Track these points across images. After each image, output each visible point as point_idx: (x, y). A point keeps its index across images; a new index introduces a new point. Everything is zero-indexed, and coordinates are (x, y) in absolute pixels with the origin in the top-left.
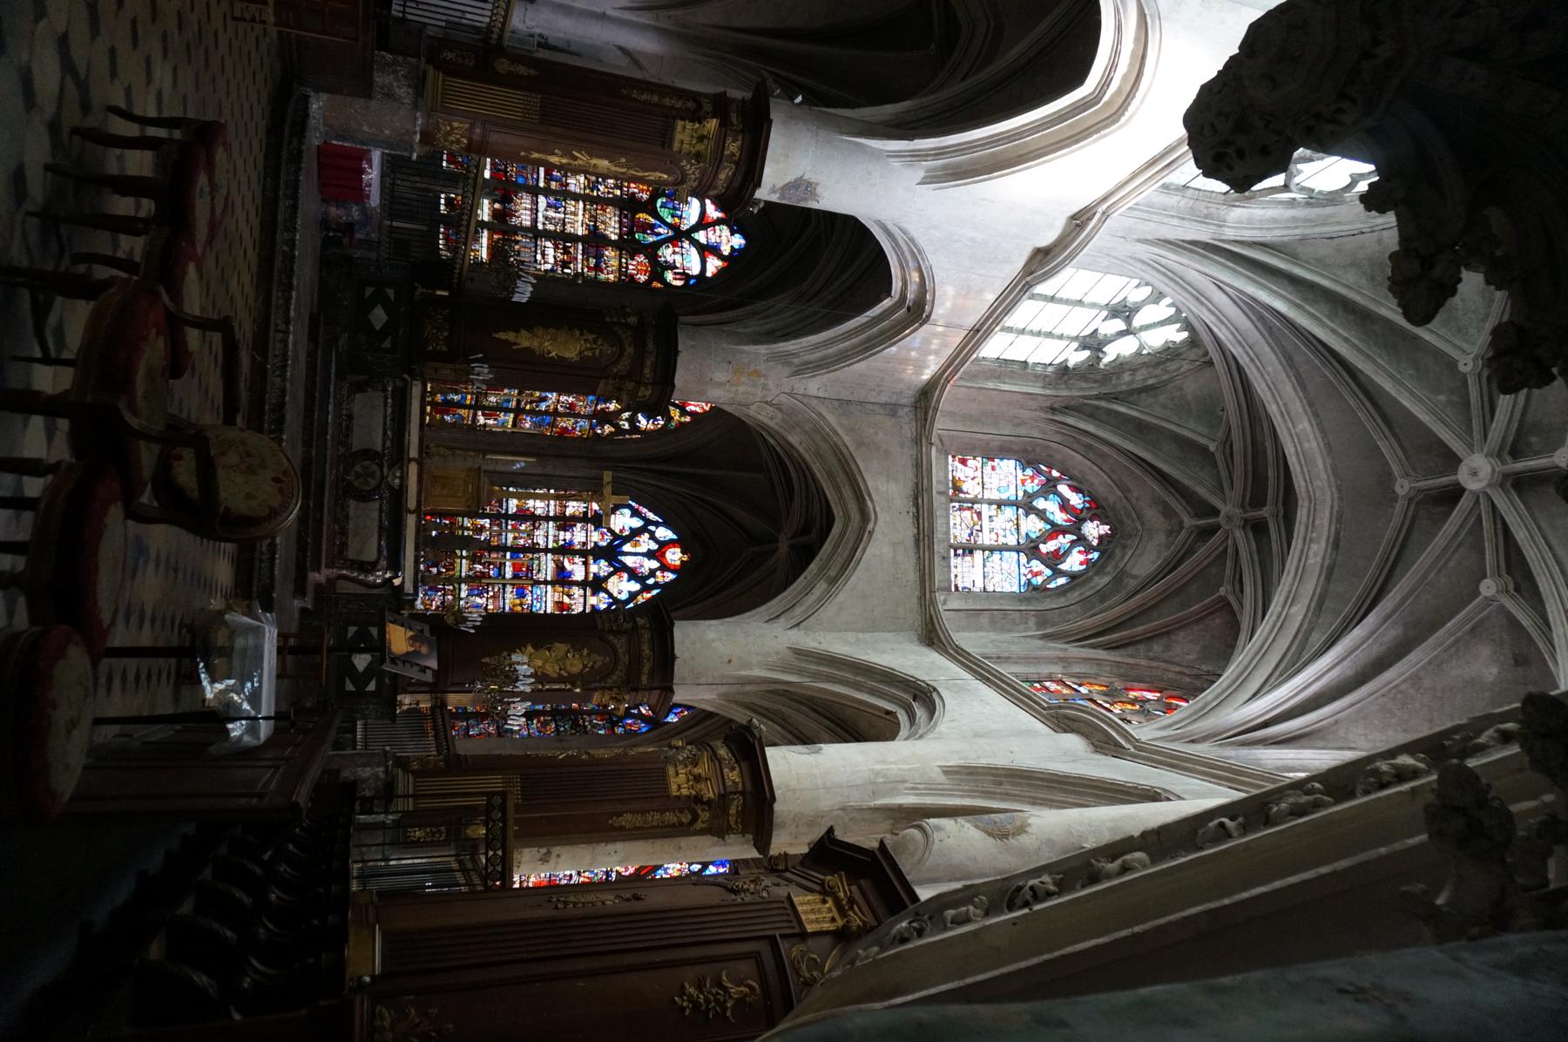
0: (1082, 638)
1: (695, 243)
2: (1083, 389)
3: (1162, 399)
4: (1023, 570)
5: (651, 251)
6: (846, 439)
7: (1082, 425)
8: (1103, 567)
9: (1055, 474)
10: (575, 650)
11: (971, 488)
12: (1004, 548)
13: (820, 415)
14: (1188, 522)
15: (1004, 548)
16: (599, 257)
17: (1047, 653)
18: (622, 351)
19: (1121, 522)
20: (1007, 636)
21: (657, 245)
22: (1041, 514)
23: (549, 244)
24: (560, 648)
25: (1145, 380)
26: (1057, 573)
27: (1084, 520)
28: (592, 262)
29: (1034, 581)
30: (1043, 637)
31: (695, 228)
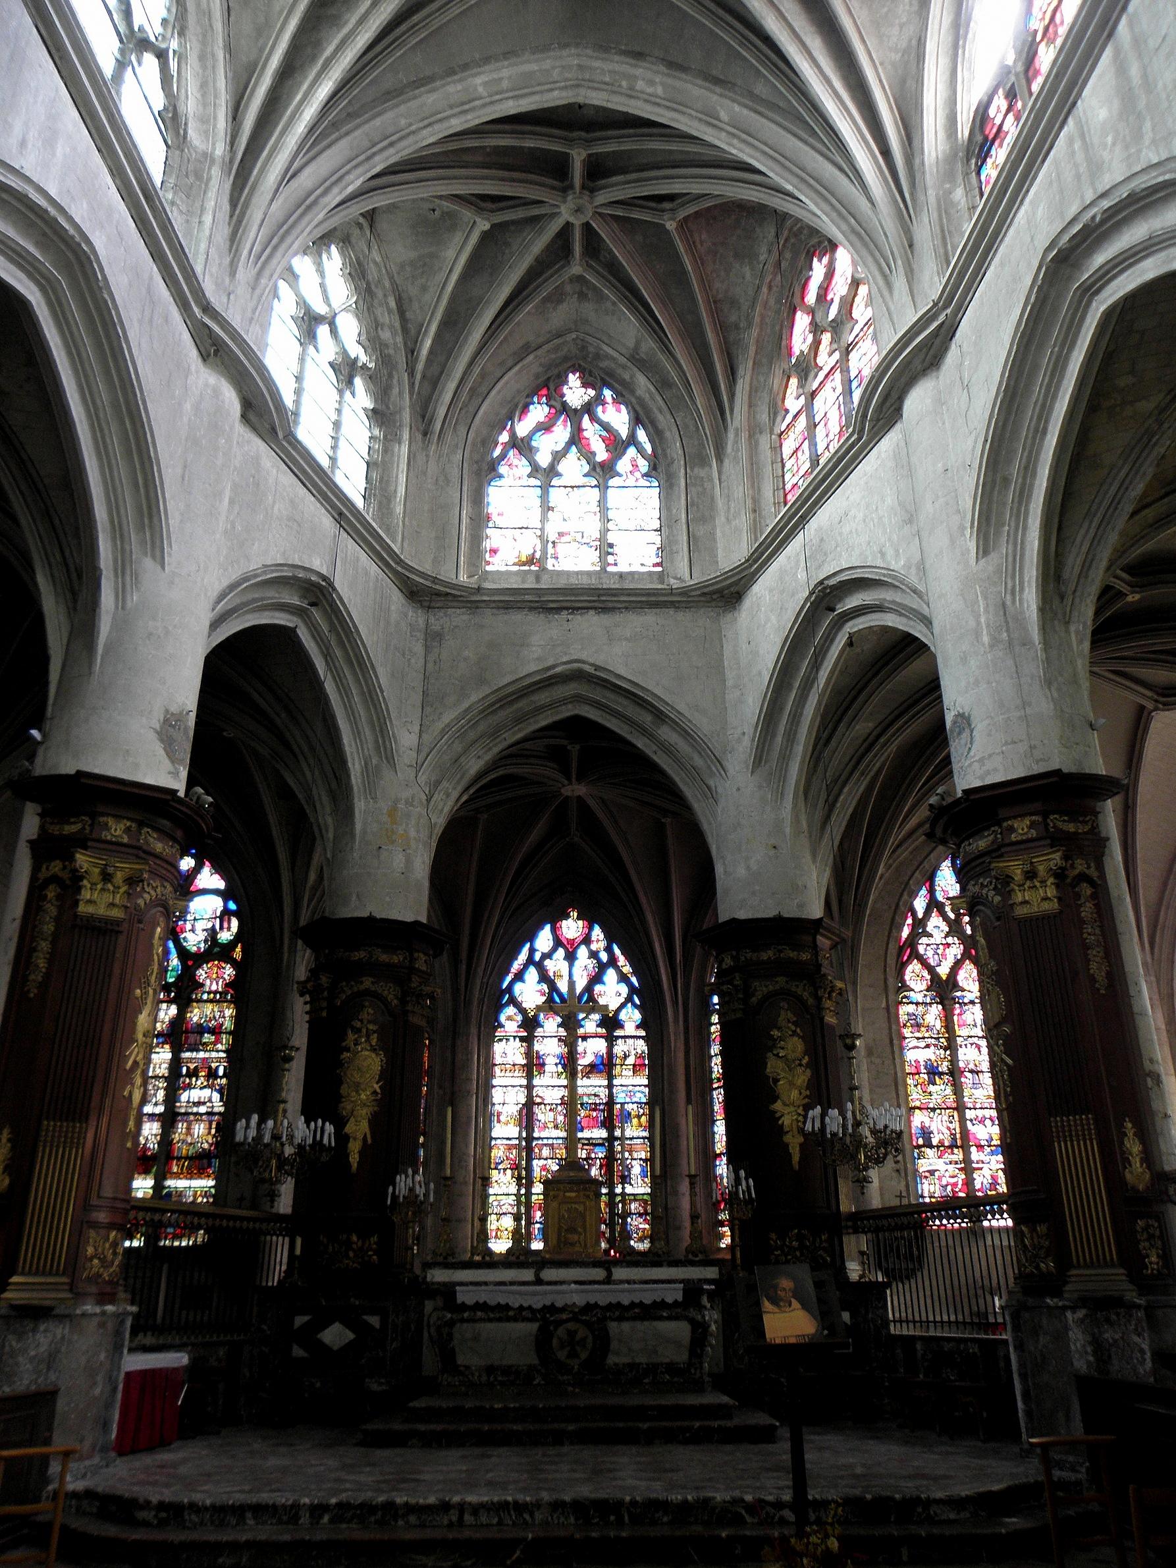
0: (721, 411)
2: (401, 393)
3: (413, 291)
4: (631, 481)
5: (192, 961)
6: (474, 697)
7: (447, 397)
8: (623, 382)
9: (504, 437)
10: (774, 1046)
11: (528, 545)
12: (602, 504)
13: (443, 732)
14: (576, 269)
15: (602, 504)
16: (201, 1029)
17: (744, 453)
18: (367, 992)
19: (566, 359)
20: (720, 503)
21: (183, 953)
22: (558, 456)
23: (184, 1097)
24: (773, 1066)
25: (390, 311)
26: (632, 440)
27: (564, 405)
28: (207, 1038)
29: (645, 469)
30: (720, 460)
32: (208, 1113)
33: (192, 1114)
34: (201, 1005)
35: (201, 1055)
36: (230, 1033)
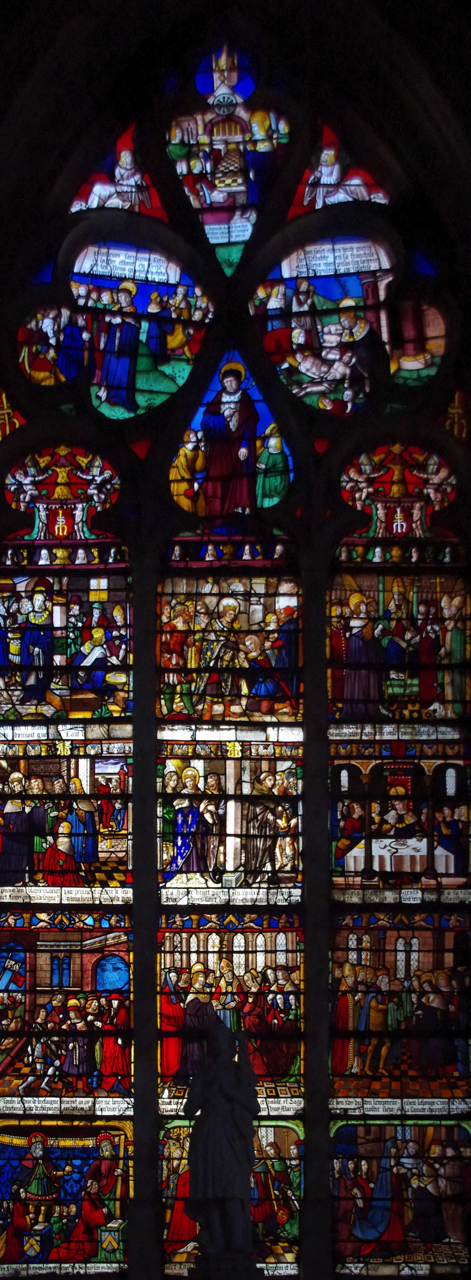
5: (322, 440)
16: (376, 657)
21: (298, 419)
31: (198, 261)
32: (423, 907)
33: (383, 907)
34: (366, 582)
35: (388, 732)
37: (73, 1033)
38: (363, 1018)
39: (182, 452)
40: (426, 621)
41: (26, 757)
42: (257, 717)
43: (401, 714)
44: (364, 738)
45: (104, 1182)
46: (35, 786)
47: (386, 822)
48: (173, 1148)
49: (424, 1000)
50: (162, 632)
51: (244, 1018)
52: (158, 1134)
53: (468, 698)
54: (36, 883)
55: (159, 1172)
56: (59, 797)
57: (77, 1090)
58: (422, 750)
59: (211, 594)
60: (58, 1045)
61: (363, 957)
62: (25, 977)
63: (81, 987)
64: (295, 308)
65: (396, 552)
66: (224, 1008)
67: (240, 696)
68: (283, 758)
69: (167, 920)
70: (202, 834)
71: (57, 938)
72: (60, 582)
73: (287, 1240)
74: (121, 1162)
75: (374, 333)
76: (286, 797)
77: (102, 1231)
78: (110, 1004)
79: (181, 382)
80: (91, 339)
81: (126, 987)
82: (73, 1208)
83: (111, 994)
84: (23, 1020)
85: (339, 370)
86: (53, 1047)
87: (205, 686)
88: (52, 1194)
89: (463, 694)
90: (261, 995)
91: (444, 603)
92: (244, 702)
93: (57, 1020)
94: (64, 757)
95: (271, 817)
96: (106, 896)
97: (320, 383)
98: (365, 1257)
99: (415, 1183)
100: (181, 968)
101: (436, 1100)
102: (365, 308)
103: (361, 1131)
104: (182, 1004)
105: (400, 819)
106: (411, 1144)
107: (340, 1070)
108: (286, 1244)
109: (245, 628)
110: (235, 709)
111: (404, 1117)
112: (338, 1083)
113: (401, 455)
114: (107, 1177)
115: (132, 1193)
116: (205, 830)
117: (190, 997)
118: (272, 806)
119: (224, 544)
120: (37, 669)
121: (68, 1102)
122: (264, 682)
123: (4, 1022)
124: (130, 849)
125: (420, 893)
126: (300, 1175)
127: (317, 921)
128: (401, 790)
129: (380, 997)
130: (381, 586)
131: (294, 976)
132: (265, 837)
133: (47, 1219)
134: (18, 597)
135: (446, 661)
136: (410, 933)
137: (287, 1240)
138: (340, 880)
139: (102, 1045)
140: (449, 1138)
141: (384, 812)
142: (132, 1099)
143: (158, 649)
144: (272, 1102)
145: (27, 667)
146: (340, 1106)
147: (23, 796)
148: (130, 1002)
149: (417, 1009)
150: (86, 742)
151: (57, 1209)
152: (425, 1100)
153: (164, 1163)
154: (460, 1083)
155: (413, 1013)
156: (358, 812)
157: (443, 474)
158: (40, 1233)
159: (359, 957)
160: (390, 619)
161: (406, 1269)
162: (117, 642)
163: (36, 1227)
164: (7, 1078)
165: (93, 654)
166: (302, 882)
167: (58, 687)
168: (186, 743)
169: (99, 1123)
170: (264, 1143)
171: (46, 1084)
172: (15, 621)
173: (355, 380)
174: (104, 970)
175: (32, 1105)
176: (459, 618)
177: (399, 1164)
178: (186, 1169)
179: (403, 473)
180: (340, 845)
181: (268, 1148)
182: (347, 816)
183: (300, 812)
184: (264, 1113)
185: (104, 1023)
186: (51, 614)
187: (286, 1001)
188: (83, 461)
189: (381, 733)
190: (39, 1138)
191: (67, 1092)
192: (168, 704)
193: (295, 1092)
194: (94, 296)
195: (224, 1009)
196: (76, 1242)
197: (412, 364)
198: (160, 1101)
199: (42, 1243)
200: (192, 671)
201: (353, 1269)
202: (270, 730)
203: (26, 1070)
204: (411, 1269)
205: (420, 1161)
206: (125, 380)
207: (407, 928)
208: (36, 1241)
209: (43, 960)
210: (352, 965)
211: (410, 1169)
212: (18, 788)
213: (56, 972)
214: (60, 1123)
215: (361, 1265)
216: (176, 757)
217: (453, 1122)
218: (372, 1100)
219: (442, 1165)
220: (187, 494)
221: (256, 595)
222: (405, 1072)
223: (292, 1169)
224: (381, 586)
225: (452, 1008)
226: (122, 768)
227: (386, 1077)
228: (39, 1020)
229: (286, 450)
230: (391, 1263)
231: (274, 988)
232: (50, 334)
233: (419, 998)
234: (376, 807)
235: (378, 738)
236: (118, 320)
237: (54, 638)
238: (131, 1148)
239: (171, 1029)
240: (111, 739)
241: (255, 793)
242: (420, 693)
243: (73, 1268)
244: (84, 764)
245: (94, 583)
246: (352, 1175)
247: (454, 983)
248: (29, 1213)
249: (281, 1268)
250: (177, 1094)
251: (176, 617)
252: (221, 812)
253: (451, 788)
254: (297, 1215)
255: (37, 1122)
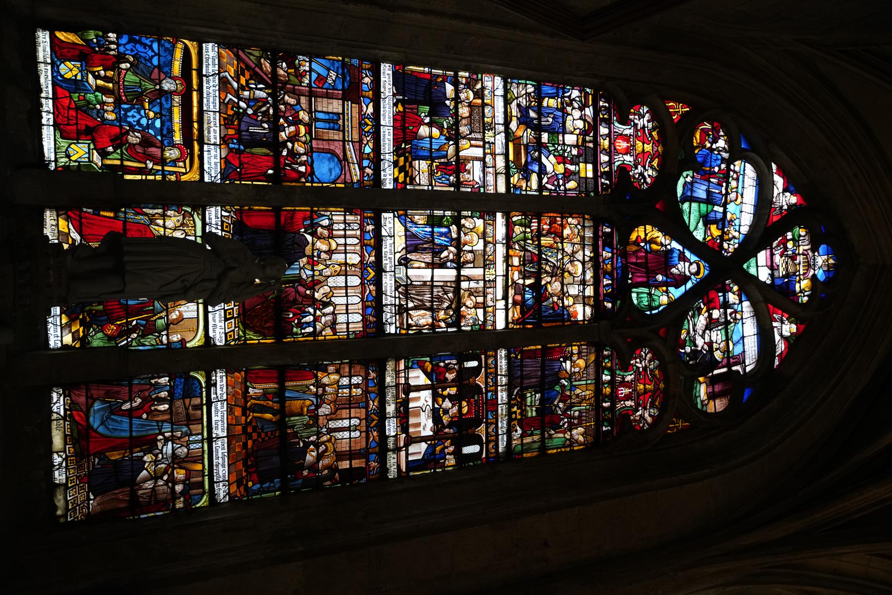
1: (750, 287)
16: (548, 381)
28: (533, 399)
31: (751, 245)
32: (383, 437)
34: (591, 370)
35: (502, 396)
36: (543, 448)
37: (276, 129)
38: (296, 395)
39: (660, 234)
40: (570, 417)
41: (484, 105)
42: (511, 292)
43: (514, 405)
44: (499, 377)
45: (140, 150)
46: (464, 111)
47: (443, 401)
48: (175, 219)
49: (312, 447)
50: (562, 218)
51: (293, 287)
52: (188, 206)
53: (525, 455)
54: (395, 105)
55: (151, 206)
56: (457, 130)
57: (227, 128)
58: (491, 423)
59: (584, 255)
60: (265, 114)
61: (345, 390)
62: (322, 88)
63: (315, 139)
64: (729, 311)
65: (608, 390)
66: (301, 269)
67: (524, 278)
68: (485, 313)
69: (370, 218)
70: (433, 248)
71: (354, 119)
72: (590, 142)
73: (86, 336)
74: (160, 168)
75: (716, 364)
76: (459, 316)
77: (89, 144)
78: (301, 164)
79: (695, 234)
80: (716, 173)
81: (315, 180)
82: (111, 117)
83: (310, 165)
84: (287, 83)
85: (700, 342)
86: (264, 109)
87: (530, 251)
88: (125, 95)
89: (527, 451)
90: (313, 302)
91: (581, 430)
92: (521, 281)
93: (287, 115)
94: (484, 136)
95: (446, 305)
96: (386, 166)
97: (694, 330)
98: (71, 416)
99: (148, 458)
100: (333, 230)
101: (226, 469)
102: (728, 358)
103: (196, 401)
104: (303, 230)
105: (446, 412)
106: (186, 450)
107: (251, 377)
108: (81, 334)
109: (565, 281)
110: (516, 276)
111: (210, 440)
112: (239, 376)
113: (659, 389)
114: (144, 153)
115: (128, 177)
116: (436, 251)
117: (309, 238)
118: (453, 306)
119: (612, 264)
120: (539, 119)
121: (214, 118)
122: (533, 297)
123: (284, 65)
124: (421, 188)
125: (394, 434)
126: (152, 345)
127: (372, 348)
128: (465, 410)
129: (313, 408)
130: (589, 382)
131: (328, 331)
132: (432, 301)
133: (99, 89)
134: (581, 109)
135: (546, 435)
136: (364, 429)
137: (86, 336)
138: (402, 367)
139: (267, 155)
140: (192, 486)
141: (451, 397)
142: (219, 181)
143: (552, 215)
144: (220, 315)
145: (539, 110)
146: (218, 379)
147: (457, 100)
148: (304, 183)
149: (304, 442)
150: (494, 155)
151: (111, 100)
152: (226, 459)
153: (160, 211)
154: (242, 489)
155: (301, 438)
156: (450, 376)
157: (649, 420)
158: (84, 79)
159: (344, 387)
160: (570, 390)
161: (60, 459)
162: (556, 183)
163: (90, 76)
164: (236, 62)
165: (550, 163)
166: (400, 334)
167: (527, 135)
168: (494, 236)
169: (196, 147)
170: (182, 309)
171: (231, 99)
172: (568, 105)
173: (695, 353)
174: (329, 160)
175: (211, 84)
176: (572, 441)
177: (166, 440)
178: (154, 232)
179: (650, 391)
180: (428, 363)
181: (177, 313)
182: (447, 368)
183: (449, 330)
184: (210, 308)
185: (286, 158)
186: (572, 133)
187: (308, 324)
188: (655, 163)
189: (502, 390)
190: (180, 88)
191: (225, 118)
192: (519, 222)
193: (230, 336)
194: (735, 176)
195: (301, 269)
196: (77, 118)
197: (702, 391)
198: (219, 208)
199: (74, 81)
200: (539, 241)
201: (58, 405)
202: (503, 302)
203: (243, 81)
204: (60, 464)
205: (170, 460)
206: (695, 195)
207: (367, 427)
208: (76, 76)
209: (335, 106)
210: (338, 381)
211: (162, 453)
212: (463, 96)
213: (327, 117)
214: (195, 110)
215: (62, 413)
216: (485, 228)
217: (207, 487)
218: (225, 409)
219: (167, 482)
220: (638, 237)
221: (584, 289)
222: (251, 438)
223: (158, 337)
224: (589, 382)
225: (305, 473)
226: (477, 183)
227: (246, 420)
228: (286, 97)
229: (661, 308)
230: (66, 444)
231: (318, 313)
232: (718, 145)
233: (313, 443)
234: (453, 391)
235: (499, 388)
236: (724, 192)
237: (558, 133)
238: (173, 178)
239: (283, 219)
240: (496, 174)
241: (462, 291)
242: (527, 417)
243: (48, 112)
244: (479, 152)
245: (590, 167)
246: (153, 397)
247: (326, 471)
248: (105, 70)
249: (55, 331)
250: (225, 224)
251: (571, 228)
252: (449, 264)
253: (468, 450)
254: (113, 344)
255: (195, 87)
